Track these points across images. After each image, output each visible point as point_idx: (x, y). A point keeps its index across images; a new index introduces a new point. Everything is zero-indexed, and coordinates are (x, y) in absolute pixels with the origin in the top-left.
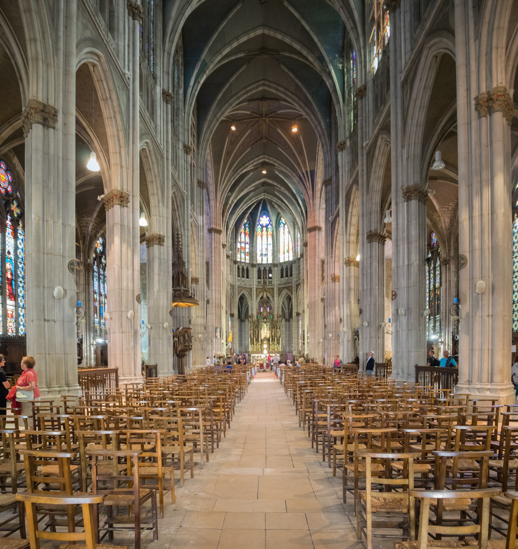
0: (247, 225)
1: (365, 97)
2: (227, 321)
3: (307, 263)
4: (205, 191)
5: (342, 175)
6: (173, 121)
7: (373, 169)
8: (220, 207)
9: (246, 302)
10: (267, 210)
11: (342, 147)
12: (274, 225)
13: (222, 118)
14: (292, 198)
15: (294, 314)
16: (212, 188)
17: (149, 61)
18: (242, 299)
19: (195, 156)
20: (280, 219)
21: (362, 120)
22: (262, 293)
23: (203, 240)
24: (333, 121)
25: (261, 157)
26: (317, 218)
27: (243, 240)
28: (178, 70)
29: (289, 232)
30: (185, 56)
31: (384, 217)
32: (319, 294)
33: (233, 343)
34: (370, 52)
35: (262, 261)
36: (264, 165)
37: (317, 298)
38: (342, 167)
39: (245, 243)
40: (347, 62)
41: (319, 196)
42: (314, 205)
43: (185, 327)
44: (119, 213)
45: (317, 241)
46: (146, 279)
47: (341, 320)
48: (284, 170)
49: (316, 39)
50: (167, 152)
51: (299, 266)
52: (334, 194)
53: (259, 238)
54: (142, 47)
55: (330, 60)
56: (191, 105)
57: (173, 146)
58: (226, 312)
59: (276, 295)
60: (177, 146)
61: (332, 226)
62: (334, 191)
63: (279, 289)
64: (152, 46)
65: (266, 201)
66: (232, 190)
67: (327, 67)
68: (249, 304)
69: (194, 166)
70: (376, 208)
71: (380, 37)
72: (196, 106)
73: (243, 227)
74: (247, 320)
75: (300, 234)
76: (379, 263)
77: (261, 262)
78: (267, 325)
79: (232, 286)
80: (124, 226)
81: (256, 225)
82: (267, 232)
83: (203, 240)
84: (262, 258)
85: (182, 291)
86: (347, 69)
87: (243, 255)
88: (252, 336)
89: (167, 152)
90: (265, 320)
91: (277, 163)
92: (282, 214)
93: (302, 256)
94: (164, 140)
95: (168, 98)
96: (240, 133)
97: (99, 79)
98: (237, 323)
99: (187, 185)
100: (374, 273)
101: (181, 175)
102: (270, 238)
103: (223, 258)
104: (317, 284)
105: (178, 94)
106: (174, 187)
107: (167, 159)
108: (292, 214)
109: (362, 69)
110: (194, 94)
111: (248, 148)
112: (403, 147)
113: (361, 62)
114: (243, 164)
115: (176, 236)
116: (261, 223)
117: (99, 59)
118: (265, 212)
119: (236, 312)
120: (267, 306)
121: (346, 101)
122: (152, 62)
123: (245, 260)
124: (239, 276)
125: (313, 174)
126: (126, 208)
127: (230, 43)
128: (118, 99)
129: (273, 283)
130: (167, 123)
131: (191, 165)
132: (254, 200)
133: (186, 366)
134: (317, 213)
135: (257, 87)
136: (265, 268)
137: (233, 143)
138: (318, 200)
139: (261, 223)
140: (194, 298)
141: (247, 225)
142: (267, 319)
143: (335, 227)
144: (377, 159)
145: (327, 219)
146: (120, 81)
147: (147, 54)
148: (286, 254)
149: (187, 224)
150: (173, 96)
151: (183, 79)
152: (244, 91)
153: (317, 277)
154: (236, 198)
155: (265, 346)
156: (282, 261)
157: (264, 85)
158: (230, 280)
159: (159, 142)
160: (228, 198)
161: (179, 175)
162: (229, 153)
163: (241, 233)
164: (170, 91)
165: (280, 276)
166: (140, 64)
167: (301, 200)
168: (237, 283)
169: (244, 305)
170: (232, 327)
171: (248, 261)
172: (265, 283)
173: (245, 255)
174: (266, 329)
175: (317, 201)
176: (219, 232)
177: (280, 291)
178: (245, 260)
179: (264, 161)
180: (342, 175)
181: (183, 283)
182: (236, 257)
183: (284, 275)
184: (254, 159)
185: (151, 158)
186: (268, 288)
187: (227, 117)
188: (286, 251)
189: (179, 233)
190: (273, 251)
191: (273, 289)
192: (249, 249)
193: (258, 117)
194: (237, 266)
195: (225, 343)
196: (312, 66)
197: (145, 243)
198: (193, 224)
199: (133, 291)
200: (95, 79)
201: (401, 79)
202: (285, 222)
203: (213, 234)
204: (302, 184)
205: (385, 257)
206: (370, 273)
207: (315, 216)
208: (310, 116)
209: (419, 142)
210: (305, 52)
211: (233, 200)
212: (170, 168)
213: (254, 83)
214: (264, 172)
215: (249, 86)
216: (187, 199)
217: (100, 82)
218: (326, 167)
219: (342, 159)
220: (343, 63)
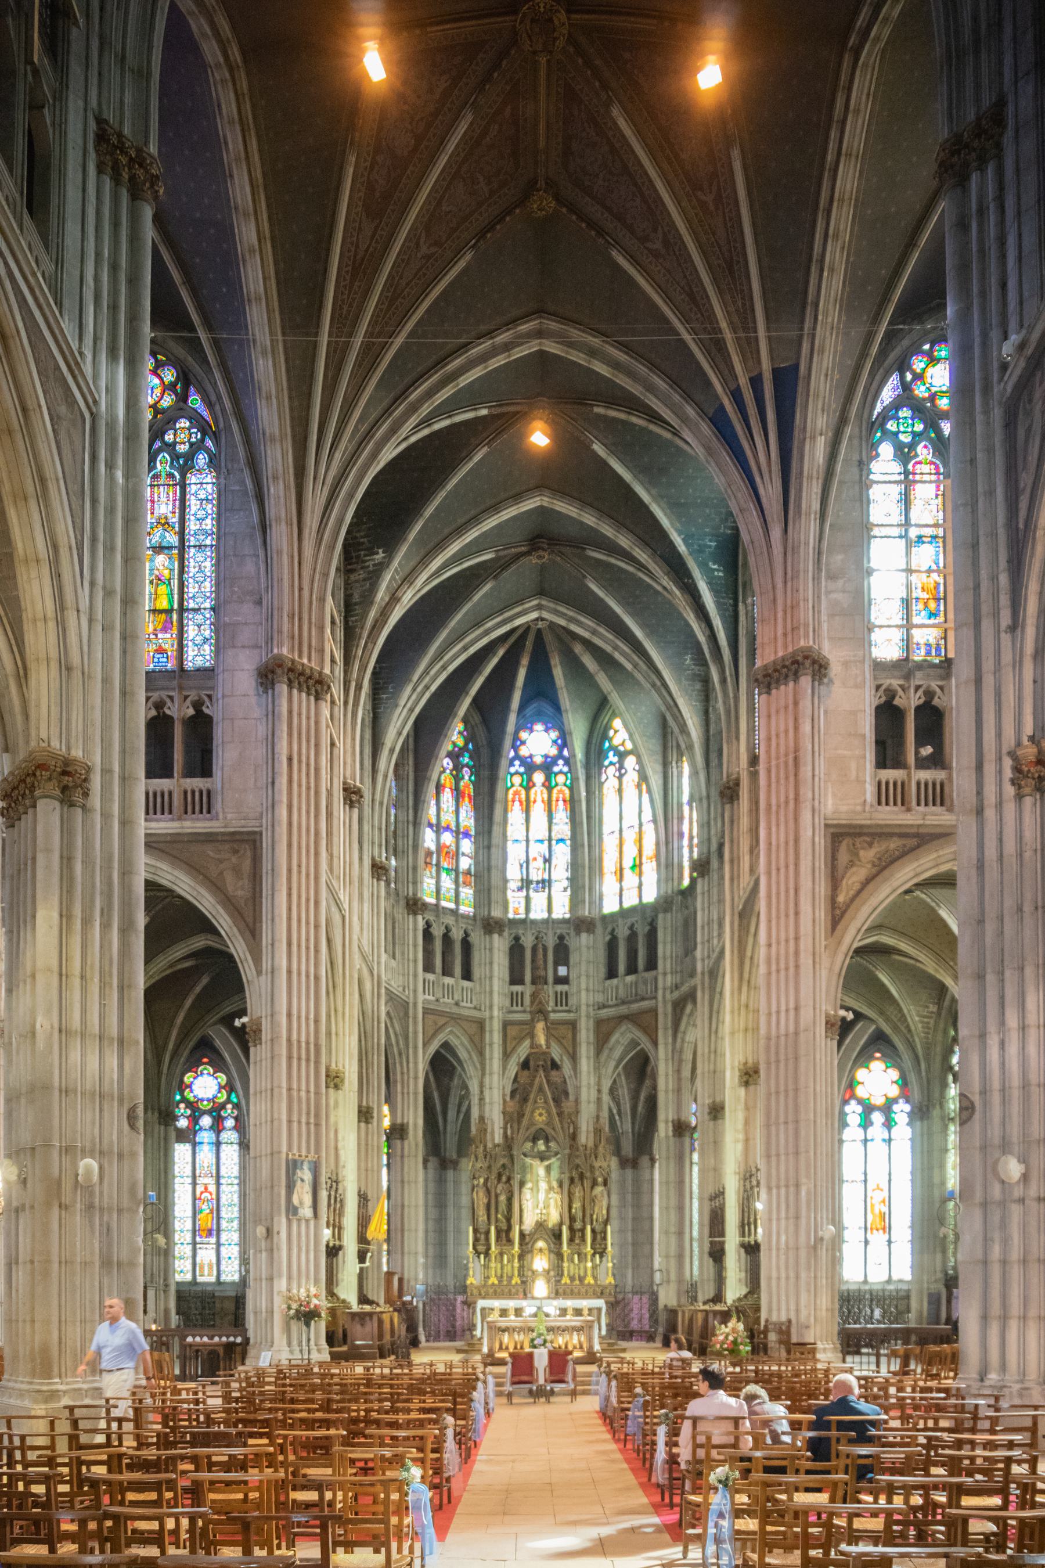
0: (466, 759)
20: (605, 736)
35: (528, 909)
39: (459, 834)
53: (516, 815)
63: (599, 1023)
68: (474, 1087)
82: (550, 789)
102: (562, 815)
116: (524, 751)
123: (457, 902)
124: (428, 967)
129: (573, 1001)
139: (524, 751)
141: (466, 759)
155: (540, 1263)
156: (610, 906)
165: (602, 971)
171: (467, 909)
173: (456, 882)
177: (603, 1032)
178: (457, 902)
183: (622, 968)
188: (628, 863)
190: (575, 865)
191: (573, 1025)
192: (475, 857)
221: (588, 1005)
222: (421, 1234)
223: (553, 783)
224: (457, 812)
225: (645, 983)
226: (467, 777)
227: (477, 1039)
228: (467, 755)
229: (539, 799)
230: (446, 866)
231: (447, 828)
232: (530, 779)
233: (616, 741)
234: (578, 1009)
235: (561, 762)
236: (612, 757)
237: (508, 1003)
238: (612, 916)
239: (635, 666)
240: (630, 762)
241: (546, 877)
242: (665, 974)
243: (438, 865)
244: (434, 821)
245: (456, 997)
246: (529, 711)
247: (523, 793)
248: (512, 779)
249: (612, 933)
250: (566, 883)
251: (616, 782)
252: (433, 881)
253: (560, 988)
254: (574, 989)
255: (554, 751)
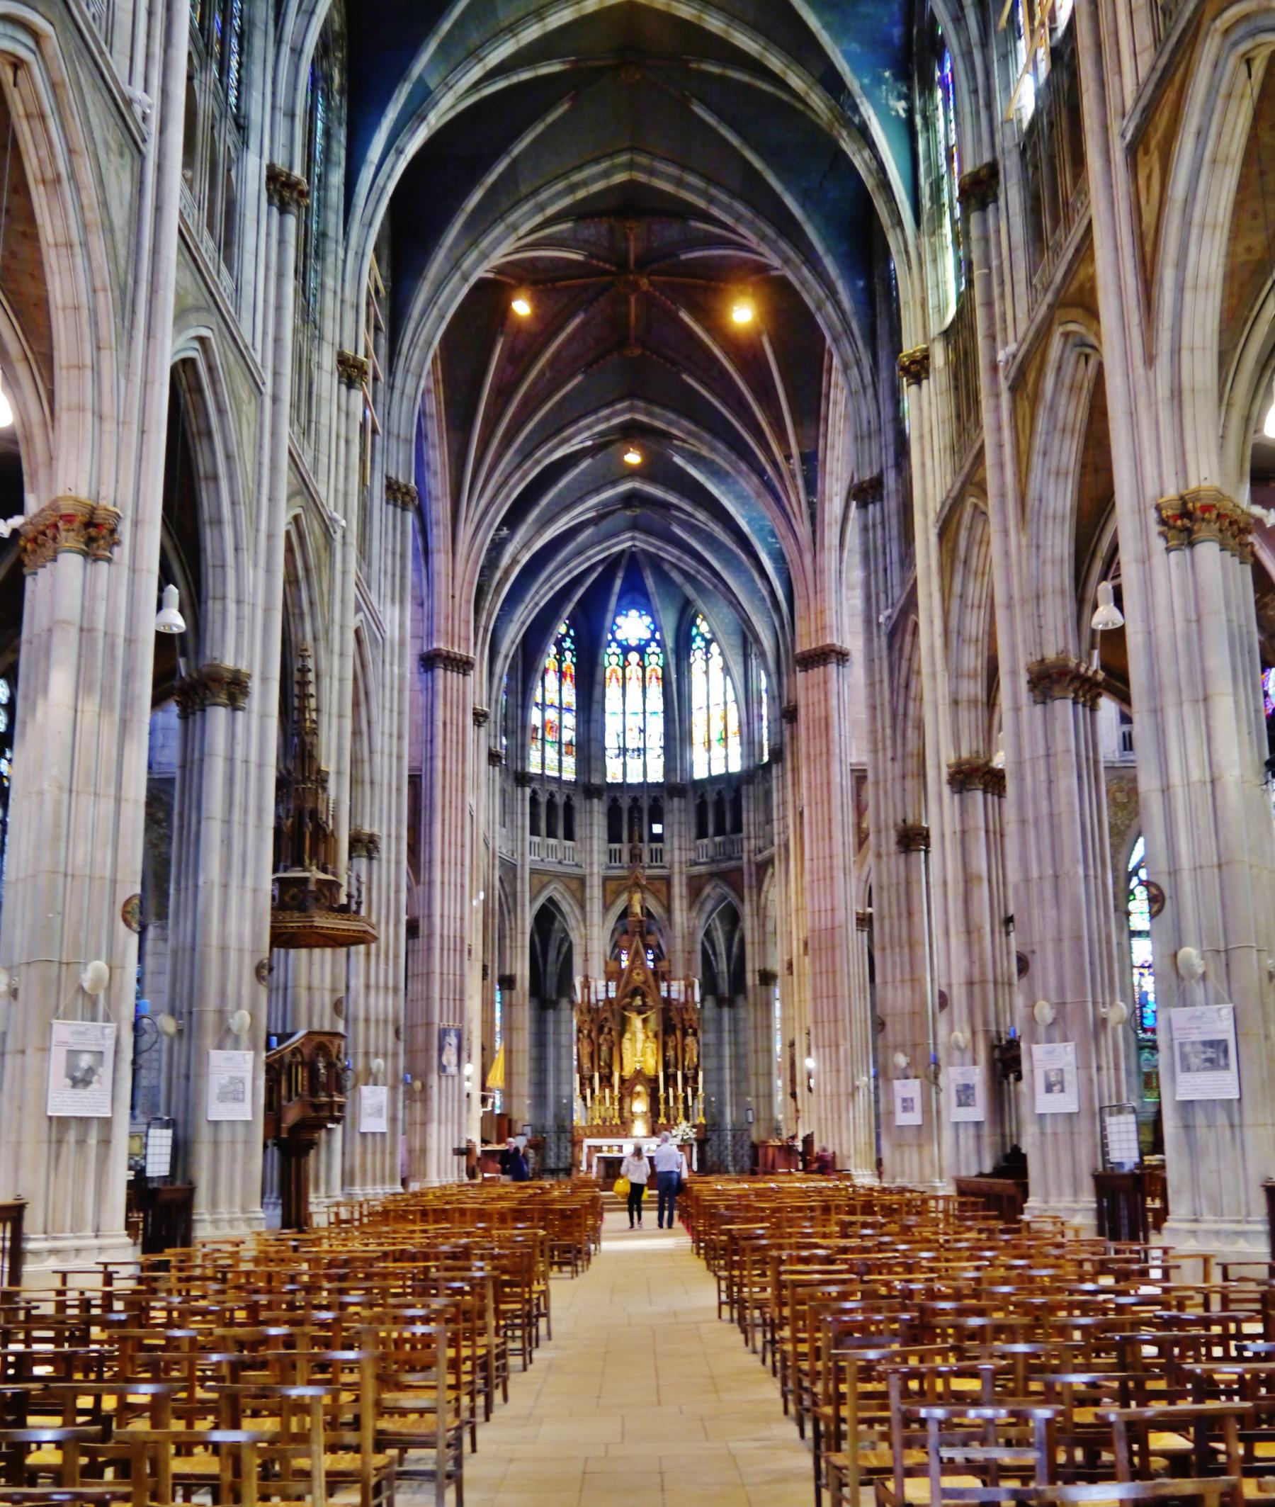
0: (568, 644)
1: (996, 200)
2: (487, 1005)
3: (796, 783)
4: (410, 516)
5: (923, 465)
6: (302, 274)
7: (1039, 442)
8: (468, 574)
9: (565, 931)
10: (646, 595)
11: (919, 369)
12: (670, 643)
13: (480, 273)
14: (734, 547)
15: (751, 979)
16: (440, 510)
17: (223, 69)
18: (547, 917)
19: (380, 398)
20: (693, 623)
21: (988, 277)
22: (625, 897)
23: (401, 691)
24: (879, 288)
25: (619, 406)
26: (831, 618)
27: (552, 697)
28: (328, 109)
29: (726, 670)
30: (350, 70)
31: (1087, 609)
32: (849, 901)
33: (508, 1094)
34: (1005, 57)
36: (631, 433)
37: (840, 914)
38: (921, 437)
40: (922, 94)
41: (836, 541)
42: (817, 571)
43: (316, 1027)
44: (78, 583)
45: (834, 702)
46: (170, 838)
47: (944, 1000)
48: (705, 452)
49: (813, 22)
50: (276, 374)
51: (768, 794)
52: (895, 532)
53: (612, 692)
54: (201, 23)
55: (862, 87)
56: (370, 225)
57: (299, 359)
58: (485, 968)
59: (679, 905)
60: (315, 357)
61: (890, 647)
62: (894, 522)
64: (236, 23)
65: (641, 558)
66: (513, 518)
67: (855, 109)
68: (575, 937)
69: (374, 431)
70: (1059, 576)
71: (1038, 10)
72: (387, 232)
73: (553, 650)
74: (564, 1003)
75: (768, 675)
76: (1080, 777)
77: (620, 780)
78: (645, 1021)
79: (509, 870)
80: (91, 630)
81: (604, 642)
82: (644, 668)
83: (401, 691)
84: (624, 764)
85: (312, 887)
86: (925, 118)
87: (551, 753)
88: (586, 1064)
89: (276, 374)
90: (638, 1001)
91: (678, 427)
92: (699, 603)
93: (777, 755)
94: (265, 333)
95: (286, 194)
96: (548, 324)
97: (33, 109)
98: (524, 1014)
99: (346, 495)
100: (1065, 817)
101: (323, 459)
102: (655, 690)
103: (477, 763)
104: (838, 861)
105: (323, 185)
106: (299, 500)
107: (275, 399)
108: (736, 604)
109: (978, 113)
110: (384, 188)
111: (572, 376)
112: (1150, 360)
113: (975, 91)
114: (553, 429)
115: (297, 676)
116: (620, 635)
117: (37, 43)
118: (636, 596)
119: (522, 969)
120: (647, 947)
121: (925, 217)
122: (234, 75)
123: (560, 770)
124: (534, 831)
125: (812, 463)
126: (103, 566)
127: (511, 30)
128: (101, 182)
129: (666, 858)
130: (280, 275)
131: (363, 426)
132: (597, 554)
133: (317, 1188)
134: (831, 599)
135: (606, 174)
136: (635, 800)
137: (519, 359)
138: (834, 555)
139: (620, 635)
140: (357, 912)
142: (644, 996)
143: (901, 649)
144: (1051, 408)
145: (869, 622)
146: (111, 122)
147: (217, 48)
148: (718, 750)
149: (342, 634)
150: (305, 187)
151: (343, 139)
152: (561, 186)
153: (837, 835)
154: (526, 545)
155: (640, 1106)
156: (700, 773)
157: (631, 166)
158: (500, 844)
159: (248, 341)
160: (497, 547)
161: (316, 459)
162: (503, 393)
163: (546, 671)
164: (298, 172)
165: (693, 834)
166: (190, 78)
167: (770, 554)
168: (528, 858)
169: (554, 943)
170: (508, 1029)
171: (569, 775)
172: (635, 857)
173: (560, 753)
174: (640, 1036)
175: (830, 559)
176: (462, 665)
177: (695, 888)
178: (560, 770)
179: (633, 421)
180: (923, 465)
181: (314, 853)
182: (524, 758)
183: (711, 830)
184: (595, 411)
185: (216, 393)
186: (649, 878)
187: (499, 270)
188: (715, 736)
189: (310, 663)
190: (668, 736)
191: (668, 880)
192: (577, 730)
193: (608, 272)
194: (528, 791)
195: (477, 1095)
196: (800, 106)
197: (173, 708)
198: (365, 635)
199: (114, 882)
200: (17, 108)
201: (1123, 136)
202: (711, 631)
203: (440, 672)
204: (770, 500)
205: (1102, 759)
206: (1051, 815)
207: (822, 612)
208: (797, 272)
209: (1208, 344)
210: (775, 63)
211: (518, 552)
212: (285, 429)
213: (597, 161)
214: (633, 458)
215: (579, 168)
216: (344, 544)
217: (37, 124)
218: (861, 438)
219: (920, 409)
220: (908, 98)
222: (527, 1077)
225: (732, 843)
227: (578, 894)
232: (626, 659)
234: (671, 867)
235: (653, 644)
237: (606, 859)
238: (702, 781)
243: (543, 739)
246: (624, 602)
247: (620, 671)
248: (611, 659)
249: (702, 796)
253: (655, 846)
254: (667, 847)
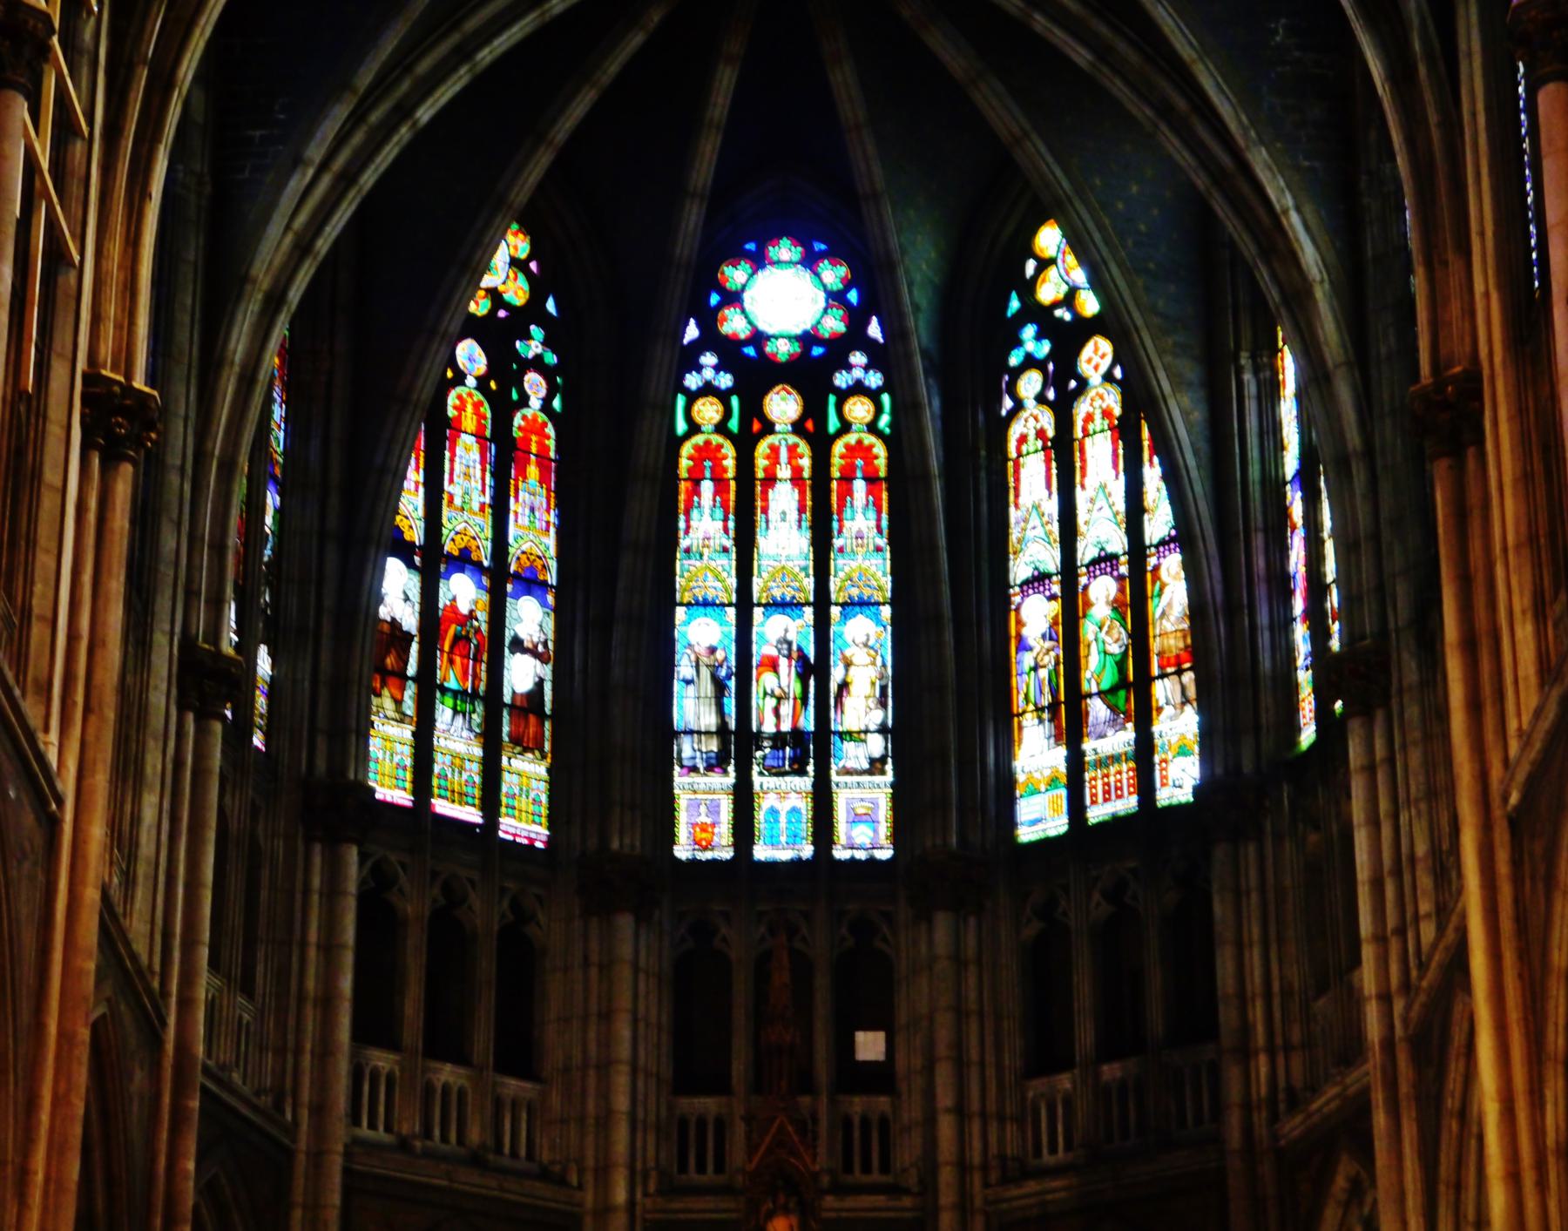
0: (533, 346)
129: (907, 1152)
141: (533, 346)
183: (1085, 1035)
221: (963, 1167)
223: (833, 424)
224: (500, 510)
226: (535, 403)
228: (536, 332)
229: (784, 472)
230: (452, 684)
231: (463, 561)
232: (753, 407)
233: (1049, 291)
234: (928, 1186)
236: (1033, 343)
239: (1103, 52)
240: (1096, 356)
241: (808, 723)
242: (1245, 1053)
244: (415, 533)
245: (474, 1135)
247: (729, 450)
250: (877, 745)
251: (1047, 421)
252: (406, 732)
253: (857, 1105)
254: (912, 1111)
255: (834, 324)
